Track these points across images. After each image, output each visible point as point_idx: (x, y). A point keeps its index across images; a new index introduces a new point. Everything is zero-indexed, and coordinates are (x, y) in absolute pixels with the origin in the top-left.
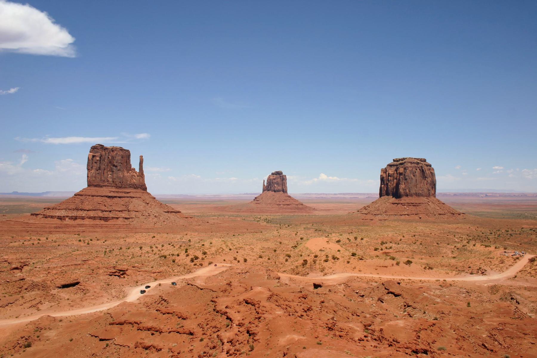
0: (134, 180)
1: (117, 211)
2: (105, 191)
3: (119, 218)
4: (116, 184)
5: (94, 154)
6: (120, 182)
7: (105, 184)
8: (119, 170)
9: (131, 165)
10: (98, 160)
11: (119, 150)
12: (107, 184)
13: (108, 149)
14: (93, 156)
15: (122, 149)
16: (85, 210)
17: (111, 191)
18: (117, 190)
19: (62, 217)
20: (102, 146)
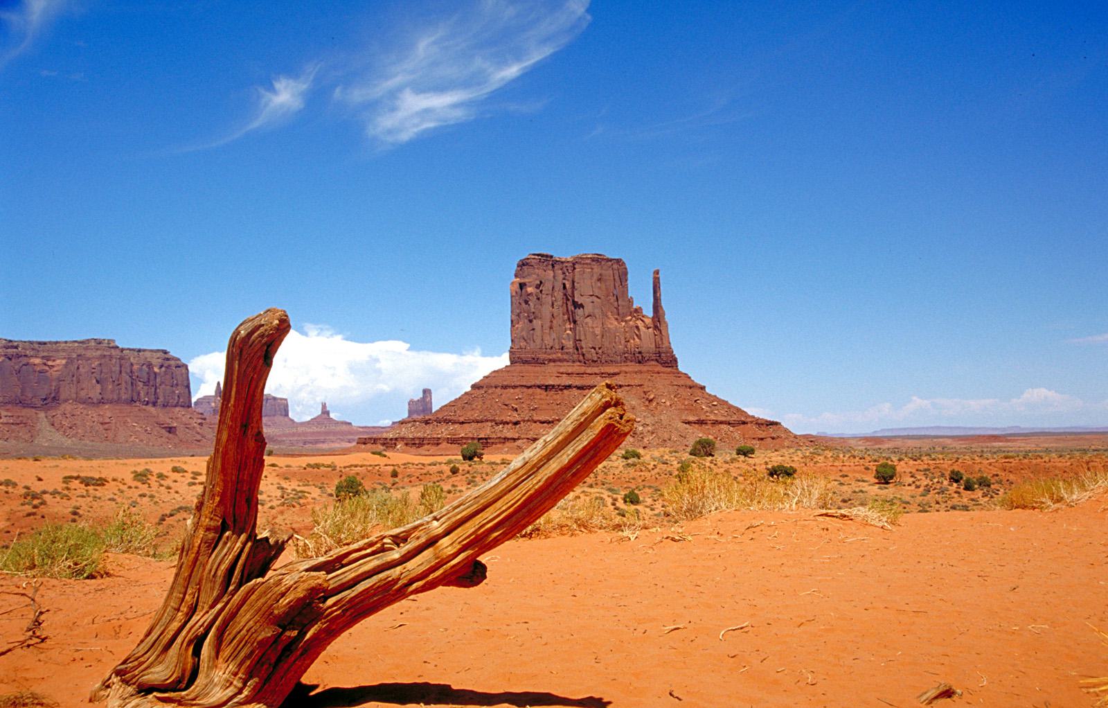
0: (637, 340)
1: (535, 422)
2: (549, 375)
3: (518, 439)
4: (583, 355)
5: (522, 281)
6: (595, 349)
7: (554, 356)
8: (588, 316)
9: (630, 301)
10: (531, 294)
11: (589, 261)
12: (560, 355)
13: (562, 262)
14: (522, 286)
15: (598, 259)
16: (454, 422)
17: (562, 373)
18: (583, 369)
19: (388, 441)
20: (545, 259)
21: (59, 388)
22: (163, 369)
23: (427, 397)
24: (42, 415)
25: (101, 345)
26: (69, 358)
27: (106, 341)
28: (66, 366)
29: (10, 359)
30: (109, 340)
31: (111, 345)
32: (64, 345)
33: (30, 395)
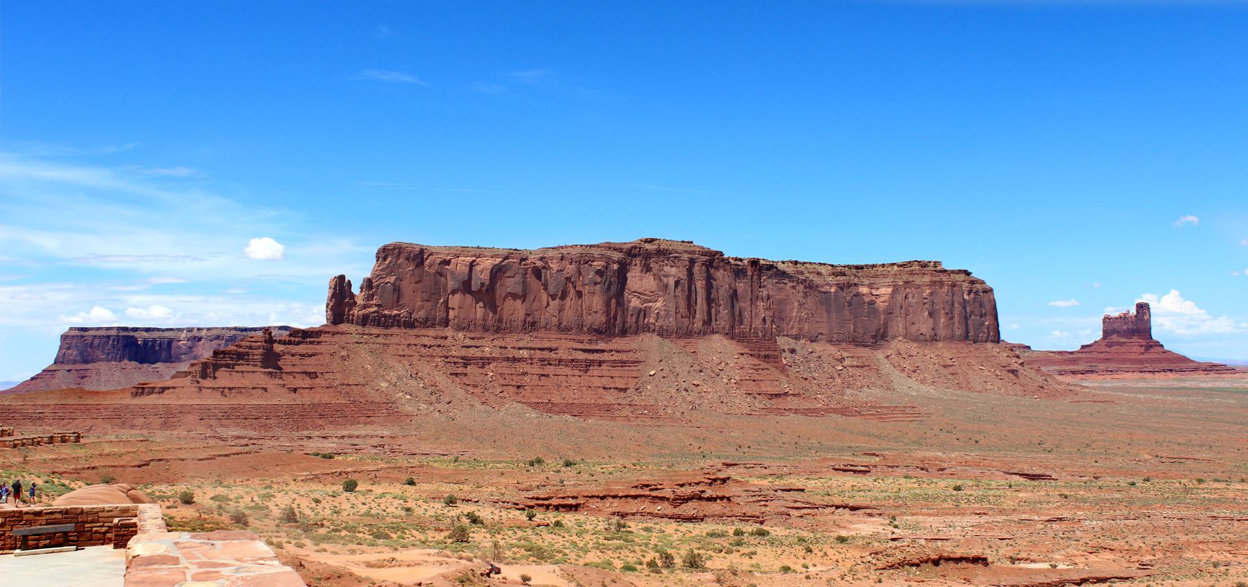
21: (887, 323)
22: (972, 295)
23: (1144, 314)
24: (880, 355)
25: (926, 269)
26: (894, 286)
27: (932, 264)
28: (893, 295)
29: (842, 289)
30: (935, 262)
31: (939, 268)
32: (881, 269)
33: (861, 331)
